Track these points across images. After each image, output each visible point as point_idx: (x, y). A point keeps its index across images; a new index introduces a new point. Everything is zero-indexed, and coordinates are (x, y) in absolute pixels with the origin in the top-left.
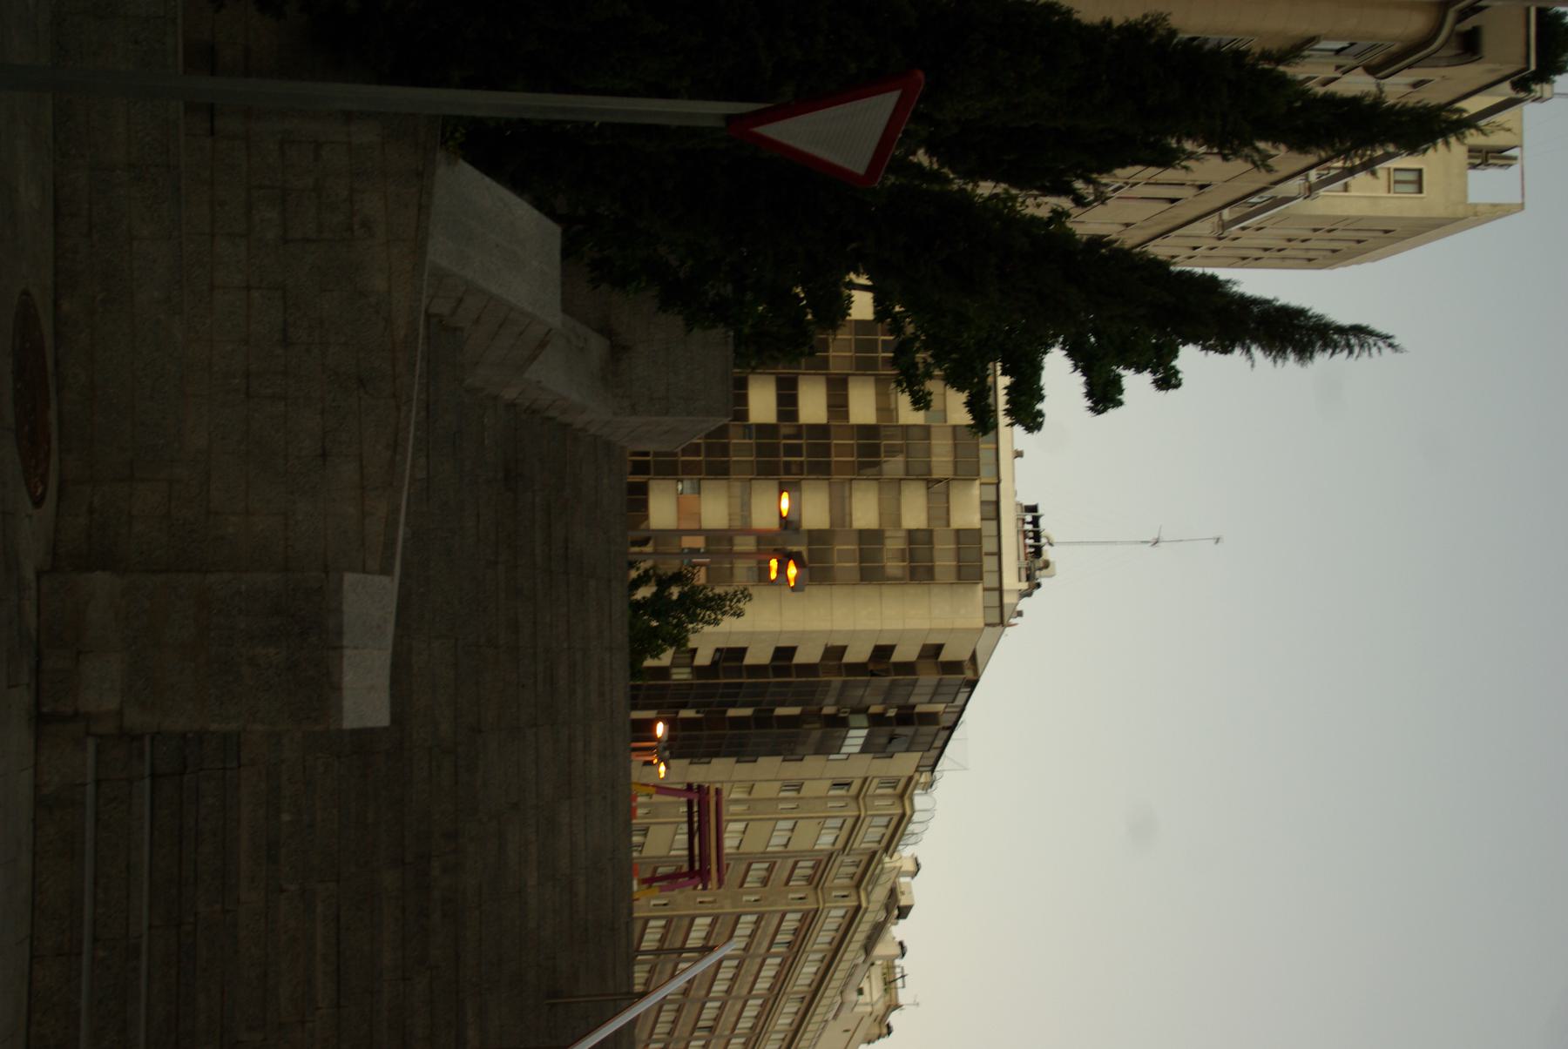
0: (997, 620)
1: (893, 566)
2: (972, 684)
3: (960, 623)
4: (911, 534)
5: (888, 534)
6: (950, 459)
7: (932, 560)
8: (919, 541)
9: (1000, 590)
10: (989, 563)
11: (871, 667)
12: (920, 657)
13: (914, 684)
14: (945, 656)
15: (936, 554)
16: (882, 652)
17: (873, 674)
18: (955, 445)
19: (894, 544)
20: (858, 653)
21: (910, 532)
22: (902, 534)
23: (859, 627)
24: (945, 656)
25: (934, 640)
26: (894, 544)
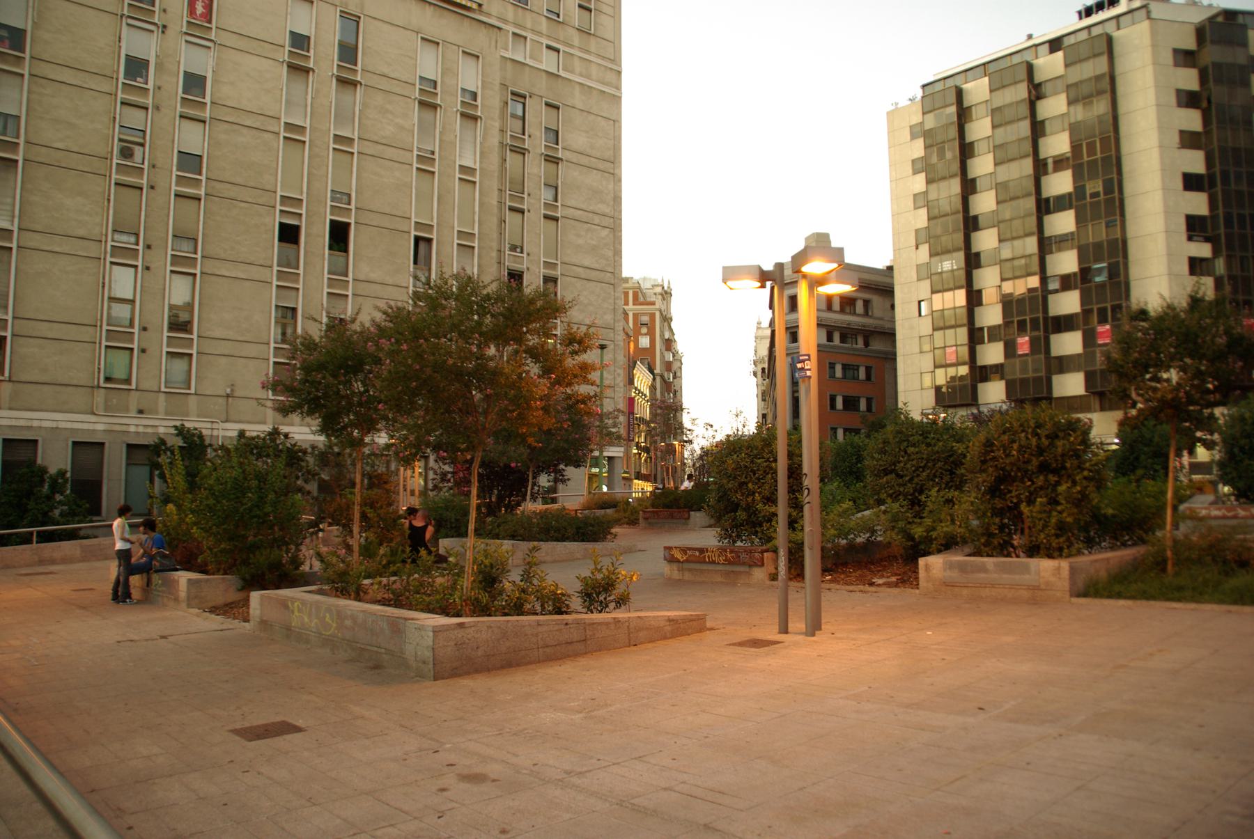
0: (1143, 12)
1: (1101, 107)
2: (1230, 15)
3: (1147, 41)
4: (1070, 103)
5: (1072, 120)
6: (1012, 88)
7: (1090, 79)
8: (1077, 96)
9: (1118, 17)
10: (1096, 31)
11: (1204, 104)
12: (1194, 66)
13: (1217, 66)
14: (1190, 44)
15: (1085, 76)
16: (1188, 99)
17: (1209, 102)
18: (1004, 87)
19: (1079, 113)
20: (1192, 120)
21: (1070, 103)
22: (1072, 108)
23: (1155, 125)
24: (1190, 44)
25: (1168, 58)
26: (1079, 113)
